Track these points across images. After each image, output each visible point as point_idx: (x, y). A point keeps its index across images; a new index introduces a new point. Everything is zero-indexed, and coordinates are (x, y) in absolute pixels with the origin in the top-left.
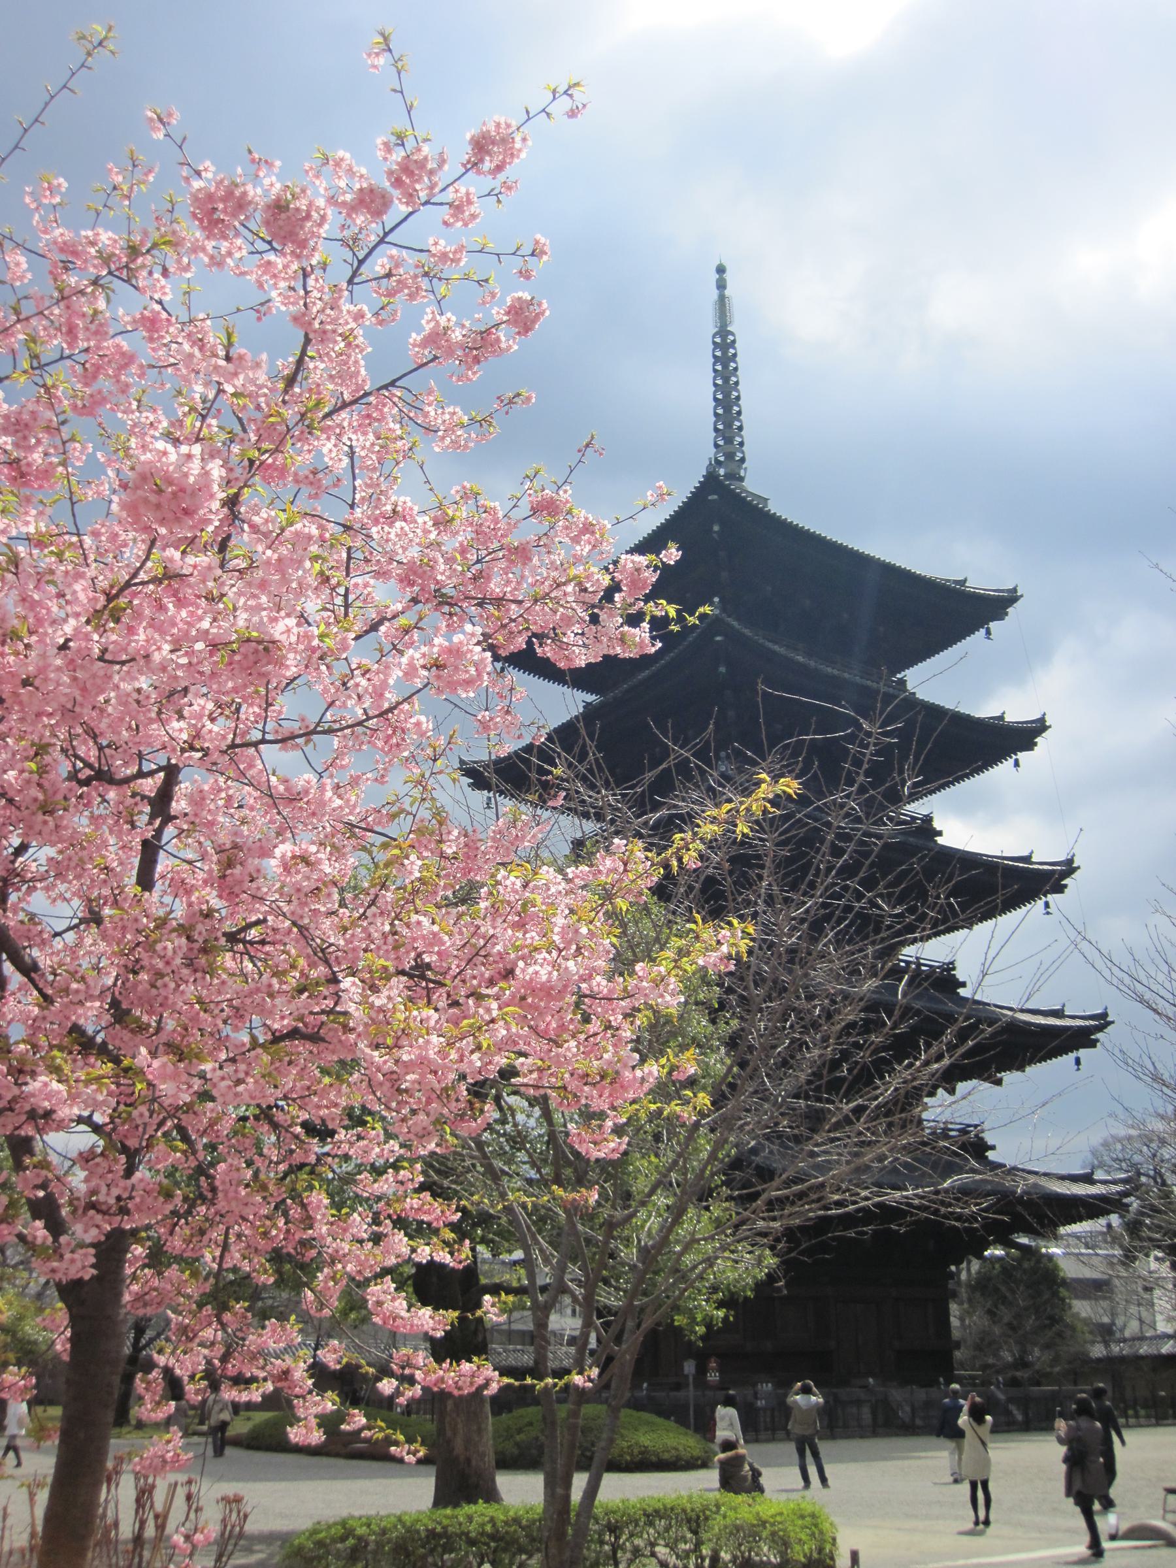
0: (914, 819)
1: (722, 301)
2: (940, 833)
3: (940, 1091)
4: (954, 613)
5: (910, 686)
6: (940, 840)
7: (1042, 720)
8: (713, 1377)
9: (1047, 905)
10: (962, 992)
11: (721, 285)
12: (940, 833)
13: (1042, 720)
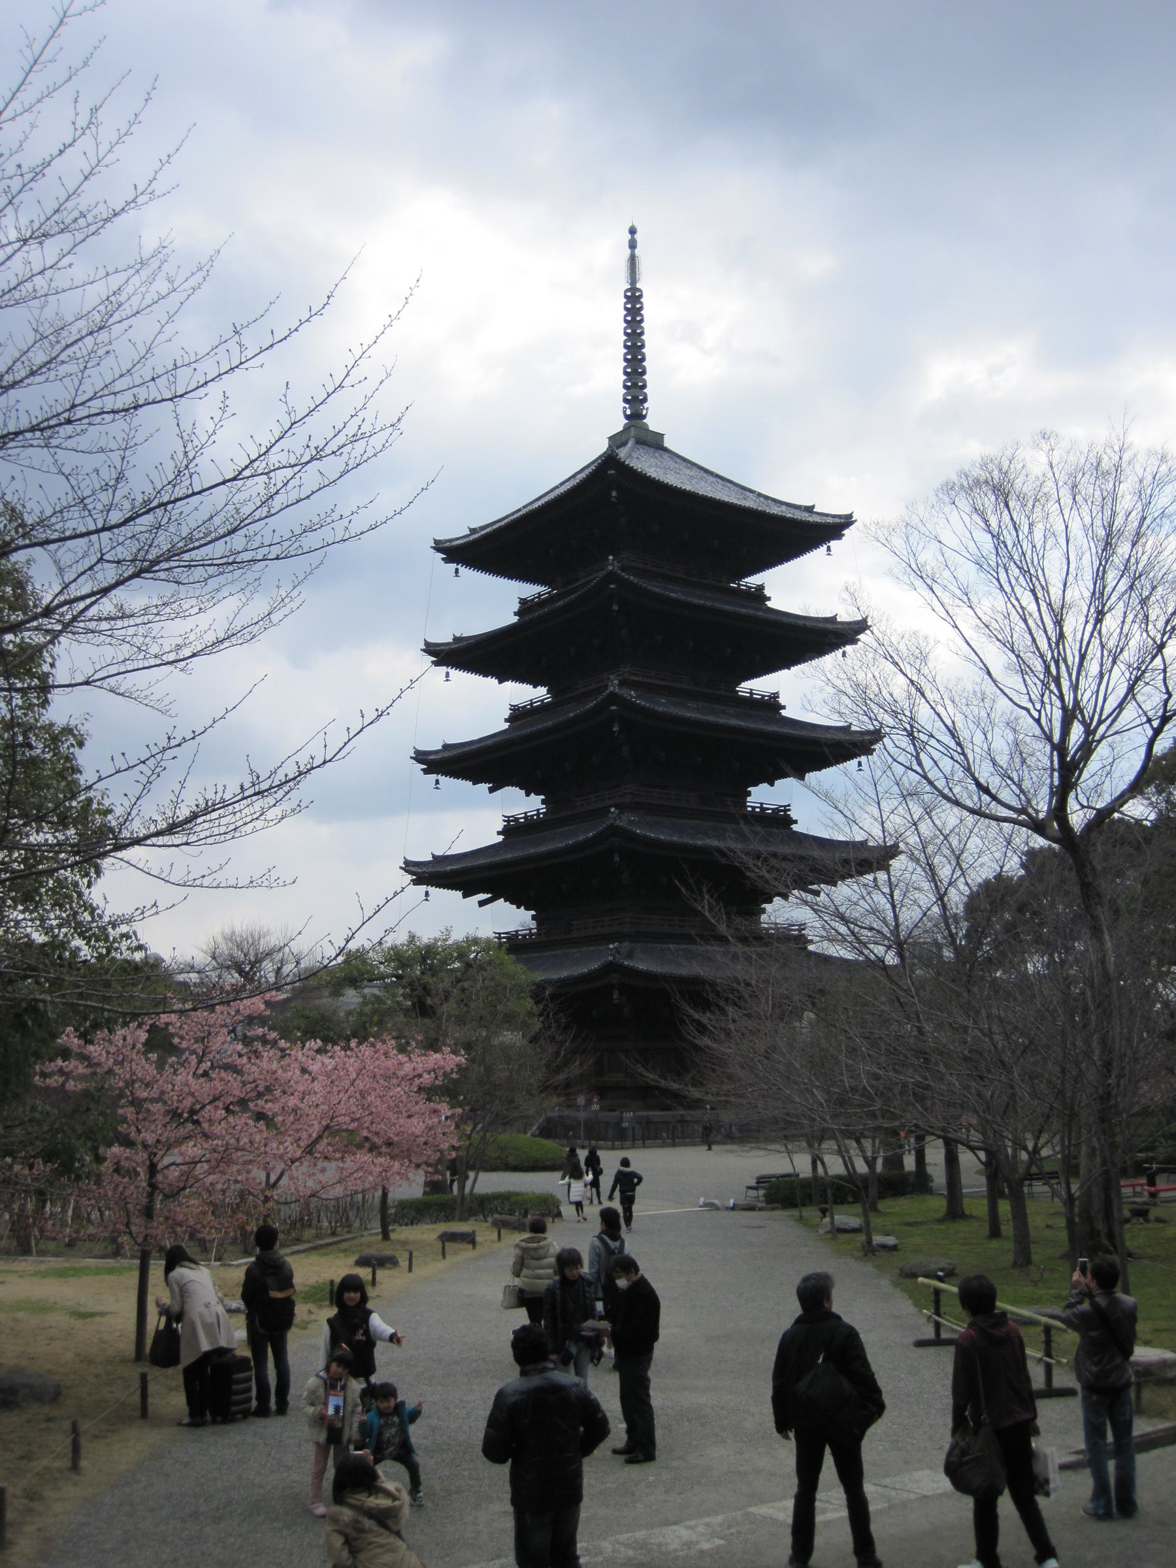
0: (763, 696)
1: (633, 260)
2: (784, 707)
3: (777, 899)
4: (804, 533)
5: (767, 592)
6: (783, 713)
7: (865, 620)
8: (596, 1107)
9: (860, 764)
10: (795, 827)
11: (633, 245)
12: (784, 707)
13: (865, 620)
